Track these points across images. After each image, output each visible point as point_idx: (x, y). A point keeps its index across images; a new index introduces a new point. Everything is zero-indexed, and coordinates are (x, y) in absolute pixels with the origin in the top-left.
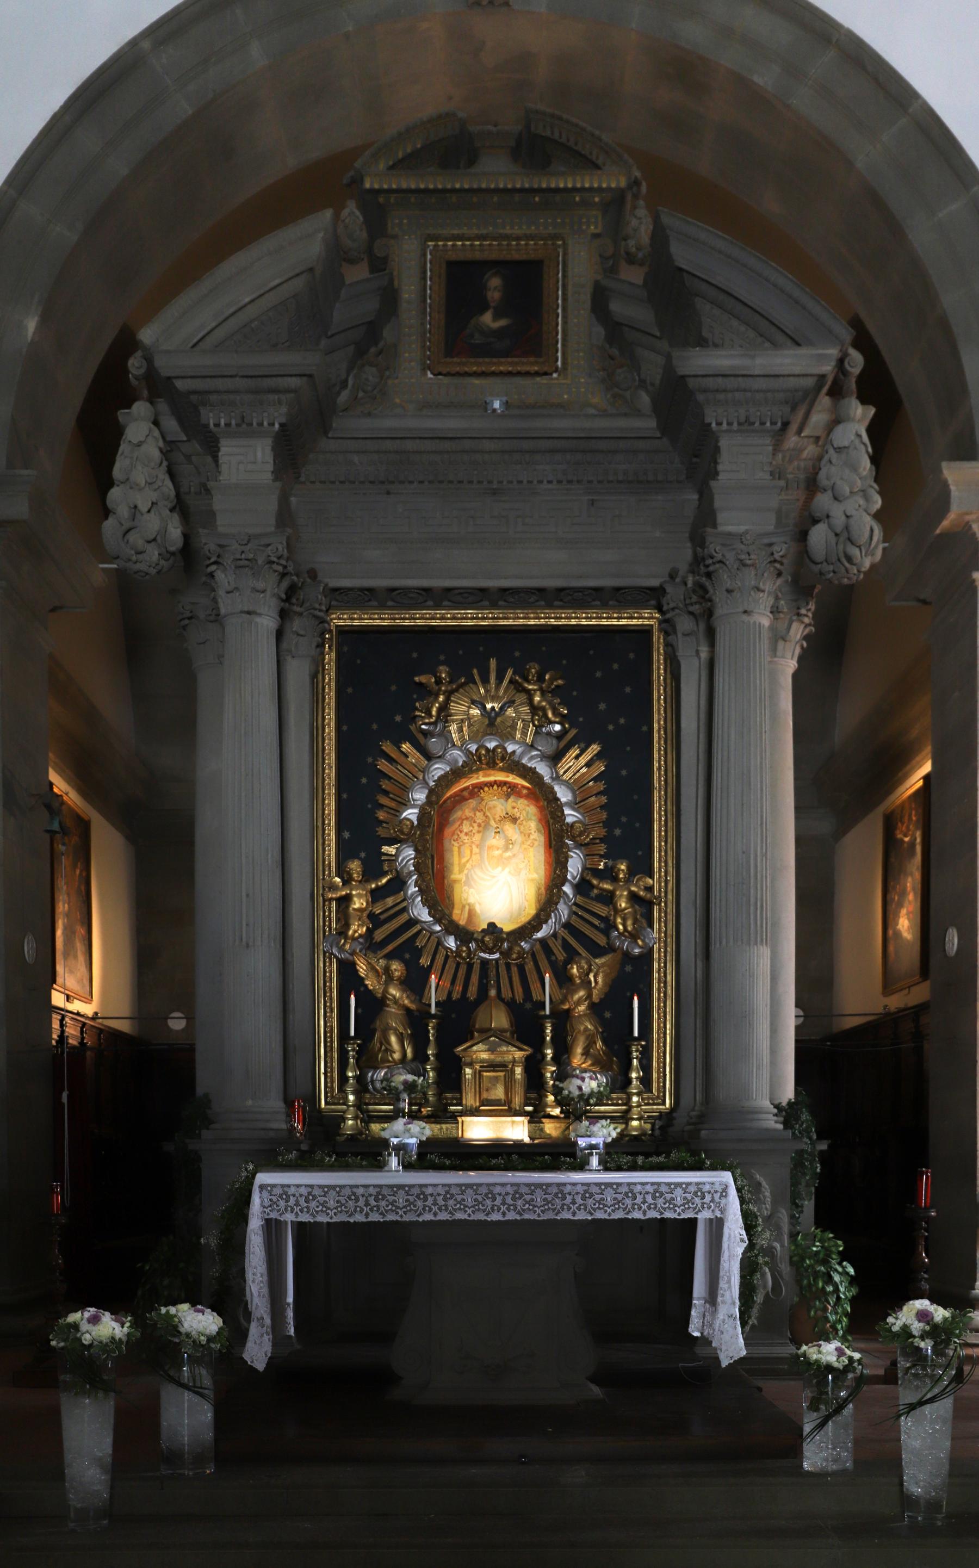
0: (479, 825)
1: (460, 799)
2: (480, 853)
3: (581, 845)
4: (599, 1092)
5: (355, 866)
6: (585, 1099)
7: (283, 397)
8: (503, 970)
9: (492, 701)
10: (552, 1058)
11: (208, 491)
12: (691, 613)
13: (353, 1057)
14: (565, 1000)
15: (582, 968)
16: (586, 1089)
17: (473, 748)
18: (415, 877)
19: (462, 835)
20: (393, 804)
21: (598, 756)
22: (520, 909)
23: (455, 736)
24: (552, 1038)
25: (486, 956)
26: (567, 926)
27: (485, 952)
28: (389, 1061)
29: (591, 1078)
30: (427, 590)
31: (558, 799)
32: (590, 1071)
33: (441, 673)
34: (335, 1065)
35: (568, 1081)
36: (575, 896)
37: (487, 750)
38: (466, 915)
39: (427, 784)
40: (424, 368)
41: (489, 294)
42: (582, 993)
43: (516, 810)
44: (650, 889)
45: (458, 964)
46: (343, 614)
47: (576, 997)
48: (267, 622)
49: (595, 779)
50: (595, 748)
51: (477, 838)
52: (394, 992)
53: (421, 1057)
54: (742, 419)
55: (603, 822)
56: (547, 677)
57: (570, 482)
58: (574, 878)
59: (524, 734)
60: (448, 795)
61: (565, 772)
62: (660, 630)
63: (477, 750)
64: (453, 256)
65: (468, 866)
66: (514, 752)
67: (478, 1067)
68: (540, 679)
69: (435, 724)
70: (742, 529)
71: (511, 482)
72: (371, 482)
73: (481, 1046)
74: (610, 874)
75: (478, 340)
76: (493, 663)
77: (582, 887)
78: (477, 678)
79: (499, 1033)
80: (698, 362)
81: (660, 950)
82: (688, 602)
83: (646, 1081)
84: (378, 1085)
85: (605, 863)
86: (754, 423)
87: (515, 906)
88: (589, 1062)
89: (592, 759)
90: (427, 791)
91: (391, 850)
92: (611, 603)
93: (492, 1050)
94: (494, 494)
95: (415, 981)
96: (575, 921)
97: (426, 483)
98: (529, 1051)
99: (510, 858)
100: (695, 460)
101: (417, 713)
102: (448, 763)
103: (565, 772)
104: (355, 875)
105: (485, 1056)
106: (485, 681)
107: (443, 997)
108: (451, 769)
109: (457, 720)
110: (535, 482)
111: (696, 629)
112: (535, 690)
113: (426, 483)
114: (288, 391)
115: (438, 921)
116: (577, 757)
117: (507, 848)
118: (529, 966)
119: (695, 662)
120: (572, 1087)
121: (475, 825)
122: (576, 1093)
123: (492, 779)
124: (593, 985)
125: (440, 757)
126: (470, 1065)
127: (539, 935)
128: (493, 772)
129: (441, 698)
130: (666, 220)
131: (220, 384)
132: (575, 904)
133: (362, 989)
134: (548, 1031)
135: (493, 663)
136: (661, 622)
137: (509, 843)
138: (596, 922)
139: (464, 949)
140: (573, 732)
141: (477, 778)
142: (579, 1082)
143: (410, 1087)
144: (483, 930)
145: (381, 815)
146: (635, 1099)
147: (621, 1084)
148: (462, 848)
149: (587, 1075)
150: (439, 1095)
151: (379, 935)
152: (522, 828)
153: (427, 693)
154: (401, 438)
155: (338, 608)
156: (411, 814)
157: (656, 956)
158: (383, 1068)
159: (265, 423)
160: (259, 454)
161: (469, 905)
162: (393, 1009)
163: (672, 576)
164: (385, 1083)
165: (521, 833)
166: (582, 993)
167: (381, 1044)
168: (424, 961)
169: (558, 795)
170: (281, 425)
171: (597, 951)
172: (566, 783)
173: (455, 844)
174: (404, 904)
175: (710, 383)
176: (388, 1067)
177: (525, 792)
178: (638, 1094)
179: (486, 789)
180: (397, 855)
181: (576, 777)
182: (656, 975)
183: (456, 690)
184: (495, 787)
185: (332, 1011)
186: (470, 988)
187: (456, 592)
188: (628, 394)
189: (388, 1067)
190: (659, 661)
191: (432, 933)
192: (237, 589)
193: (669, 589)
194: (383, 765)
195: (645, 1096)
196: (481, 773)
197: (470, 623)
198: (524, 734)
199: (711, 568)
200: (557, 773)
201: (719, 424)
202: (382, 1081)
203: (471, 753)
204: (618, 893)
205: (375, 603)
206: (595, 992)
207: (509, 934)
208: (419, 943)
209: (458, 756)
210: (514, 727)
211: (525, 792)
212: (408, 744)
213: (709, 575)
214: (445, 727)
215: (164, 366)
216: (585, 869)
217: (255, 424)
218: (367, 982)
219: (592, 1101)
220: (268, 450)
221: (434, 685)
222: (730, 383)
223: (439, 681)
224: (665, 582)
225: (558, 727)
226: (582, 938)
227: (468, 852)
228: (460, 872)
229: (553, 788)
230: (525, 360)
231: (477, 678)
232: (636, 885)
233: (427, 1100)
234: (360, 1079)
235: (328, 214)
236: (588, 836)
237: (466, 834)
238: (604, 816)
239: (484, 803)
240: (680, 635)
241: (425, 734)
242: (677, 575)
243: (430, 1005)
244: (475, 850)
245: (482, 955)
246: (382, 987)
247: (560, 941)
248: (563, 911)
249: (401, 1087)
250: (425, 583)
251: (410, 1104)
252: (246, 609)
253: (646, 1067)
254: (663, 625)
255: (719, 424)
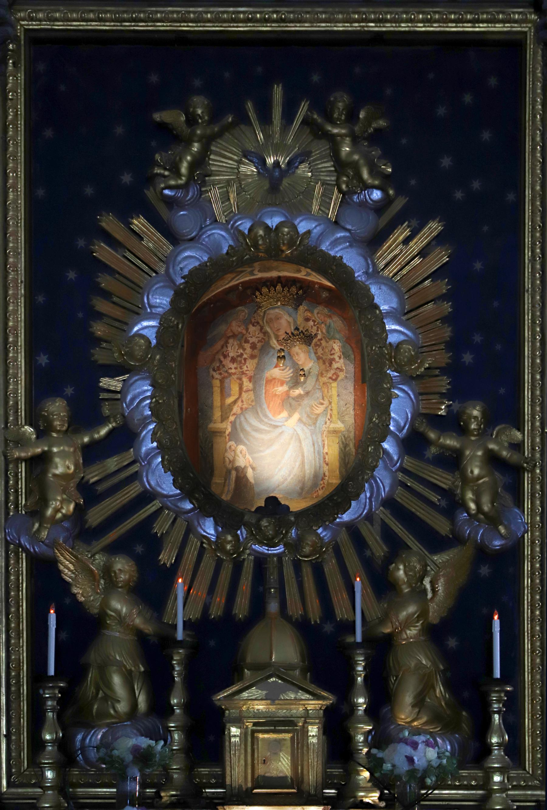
0: (253, 347)
1: (225, 305)
3: (412, 378)
4: (440, 766)
5: (57, 409)
6: (419, 777)
8: (289, 571)
9: (276, 154)
10: (365, 710)
13: (53, 710)
14: (384, 619)
15: (413, 569)
16: (419, 761)
17: (245, 225)
18: (152, 427)
19: (227, 362)
20: (117, 312)
21: (439, 239)
22: (316, 476)
23: (217, 208)
24: (365, 679)
25: (264, 549)
26: (390, 503)
27: (261, 543)
28: (110, 716)
29: (427, 744)
31: (377, 307)
32: (426, 732)
33: (195, 108)
34: (24, 722)
35: (391, 747)
36: (400, 457)
37: (267, 228)
38: (233, 485)
39: (173, 282)
42: (412, 609)
43: (311, 323)
44: (517, 447)
45: (219, 563)
47: (403, 614)
49: (434, 276)
50: (434, 227)
52: (119, 605)
53: (160, 708)
55: (446, 343)
56: (362, 115)
58: (401, 429)
59: (325, 204)
60: (205, 299)
61: (387, 265)
63: (250, 230)
65: (236, 409)
66: (309, 232)
67: (250, 725)
68: (352, 116)
69: (185, 187)
73: (254, 692)
74: (455, 424)
77: (413, 443)
78: (252, 115)
79: (282, 672)
81: (533, 542)
83: (514, 750)
84: (93, 754)
85: (448, 406)
87: (309, 471)
88: (424, 719)
89: (429, 244)
90: (172, 293)
91: (114, 383)
93: (271, 698)
95: (152, 589)
96: (401, 496)
98: (329, 699)
99: (300, 396)
101: (157, 171)
102: (206, 249)
103: (387, 265)
104: (57, 423)
105: (260, 706)
106: (265, 118)
107: (195, 614)
108: (210, 259)
109: (220, 182)
112: (341, 136)
115: (187, 494)
116: (406, 241)
117: (295, 383)
118: (331, 567)
120: (396, 758)
121: (247, 346)
122: (403, 767)
123: (274, 274)
124: (430, 595)
125: (192, 239)
126: (238, 721)
127: (346, 517)
128: (275, 264)
129: (196, 147)
132: (402, 470)
133: (68, 601)
134: (360, 668)
137: (299, 375)
138: (435, 498)
139: (229, 538)
140: (400, 203)
141: (252, 273)
142: (408, 750)
143: (143, 757)
144: (259, 509)
145: (99, 329)
146: (497, 778)
147: (476, 753)
149: (420, 739)
150: (190, 769)
151: (96, 516)
152: (320, 351)
153: (169, 136)
156: (147, 327)
157: (527, 551)
158: (100, 727)
161: (237, 469)
162: (115, 633)
164: (103, 751)
165: (319, 358)
166: (412, 609)
167: (98, 690)
168: (167, 557)
169: (377, 300)
171: (435, 542)
172: (389, 282)
173: (216, 375)
174: (135, 468)
176: (108, 725)
177: (325, 295)
178: (501, 771)
179: (265, 290)
180: (123, 392)
181: (404, 272)
182: (527, 581)
183: (220, 135)
184: (279, 287)
185: (19, 636)
186: (238, 600)
189: (108, 725)
191: (179, 513)
194: (102, 251)
195: (513, 773)
196: (256, 265)
198: (325, 204)
200: (374, 265)
202: (98, 748)
203: (242, 233)
204: (468, 452)
206: (433, 607)
207: (300, 514)
208: (159, 528)
209: (221, 239)
210: (309, 193)
211: (325, 295)
212: (142, 219)
214: (201, 193)
216: (416, 415)
218: (75, 590)
219: (429, 781)
221: (184, 127)
223: (192, 120)
225: (377, 195)
226: (412, 525)
227: (235, 388)
228: (224, 418)
229: (369, 289)
231: (252, 115)
232: (496, 441)
233: (169, 778)
234: (64, 745)
236: (422, 363)
237: (233, 360)
238: (447, 332)
239: (261, 312)
241: (170, 203)
243: (175, 627)
244: (247, 384)
245: (257, 547)
246: (99, 598)
247: (377, 526)
248: (383, 480)
249: (129, 758)
251: (144, 785)
253: (514, 727)
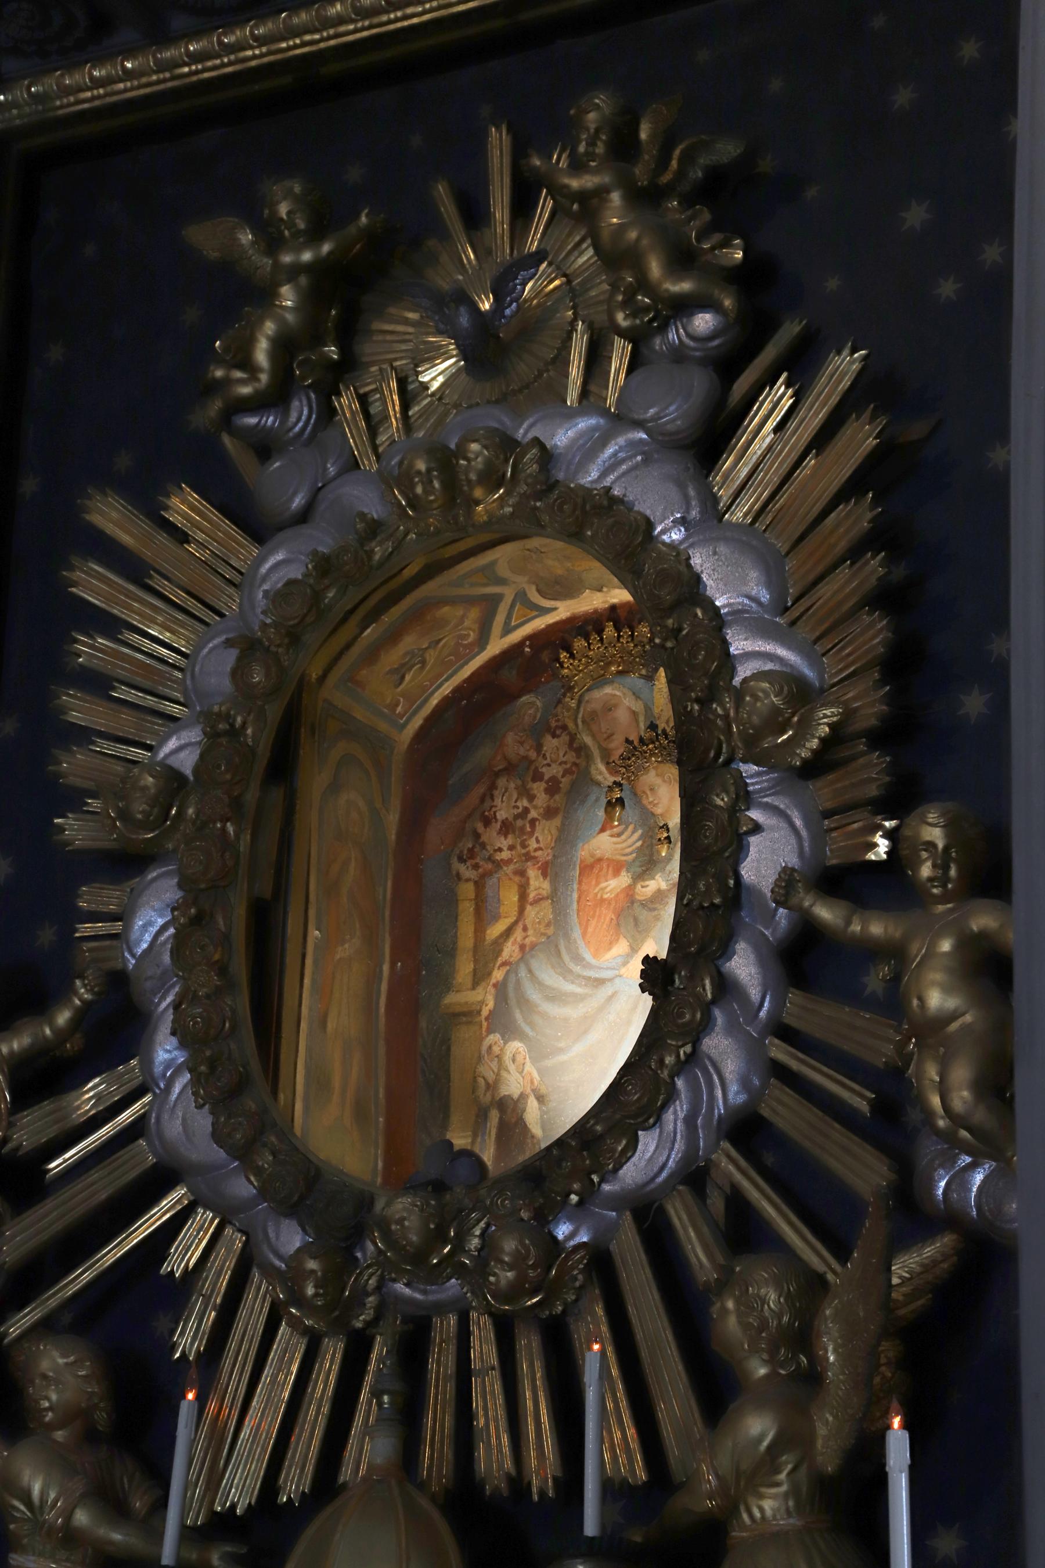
2: (553, 896)
51: (544, 836)
65: (510, 950)
121: (538, 788)
148: (491, 882)
173: (466, 871)
227: (510, 898)
228: (479, 977)
237: (506, 828)
244: (539, 885)
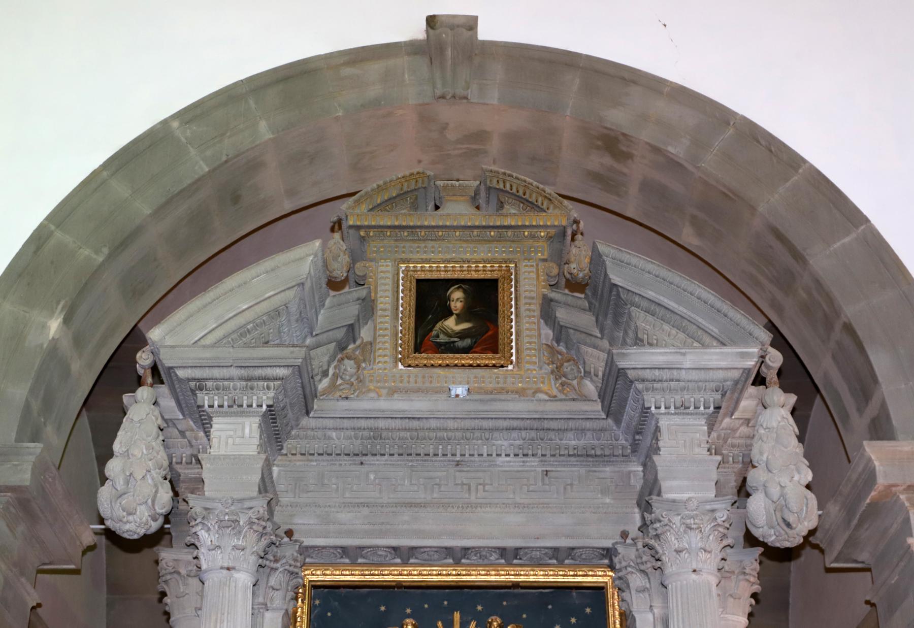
7: (271, 384)
11: (199, 461)
12: (643, 571)
30: (395, 549)
40: (396, 360)
41: (453, 305)
46: (316, 570)
48: (244, 578)
54: (678, 405)
57: (525, 455)
62: (614, 587)
64: (422, 276)
70: (685, 496)
71: (473, 455)
72: (346, 455)
75: (443, 339)
76: (457, 616)
80: (635, 359)
82: (639, 561)
86: (689, 408)
92: (567, 561)
94: (457, 465)
97: (396, 456)
100: (637, 437)
110: (494, 455)
111: (648, 586)
113: (396, 456)
114: (275, 379)
119: (650, 617)
130: (602, 248)
131: (216, 373)
135: (457, 616)
136: (614, 580)
154: (375, 418)
155: (311, 564)
159: (254, 405)
160: (247, 431)
163: (624, 535)
170: (268, 406)
175: (647, 374)
187: (422, 550)
188: (575, 382)
190: (614, 616)
192: (219, 547)
193: (620, 549)
197: (435, 579)
199: (659, 532)
201: (658, 408)
205: (347, 561)
213: (657, 537)
215: (167, 360)
217: (245, 405)
220: (255, 426)
222: (666, 375)
224: (617, 543)
230: (484, 356)
235: (317, 243)
240: (633, 592)
242: (627, 537)
250: (394, 542)
252: (226, 565)
254: (617, 582)
255: (658, 408)
